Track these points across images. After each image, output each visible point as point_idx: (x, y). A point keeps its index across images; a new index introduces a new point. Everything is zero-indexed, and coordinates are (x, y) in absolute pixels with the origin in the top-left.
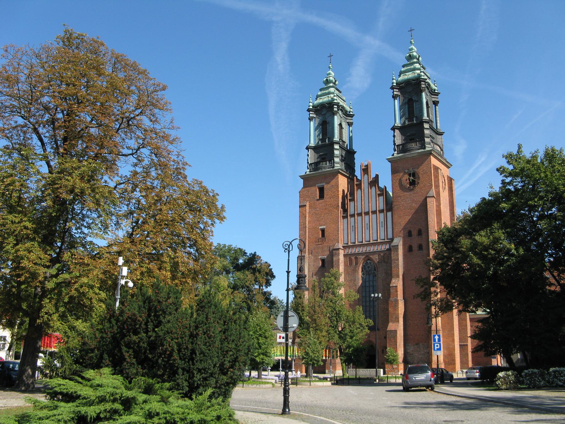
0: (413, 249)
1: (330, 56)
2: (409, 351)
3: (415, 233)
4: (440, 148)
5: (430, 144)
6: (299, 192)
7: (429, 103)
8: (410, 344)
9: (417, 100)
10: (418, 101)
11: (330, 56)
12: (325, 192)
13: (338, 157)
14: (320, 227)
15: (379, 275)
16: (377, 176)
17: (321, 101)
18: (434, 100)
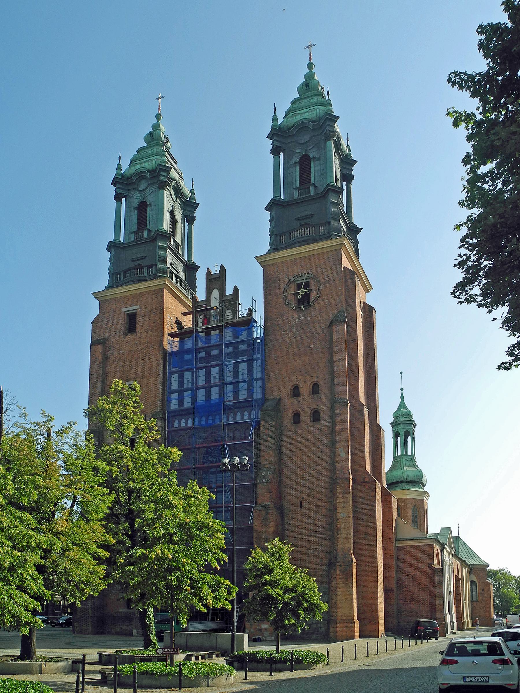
0: (302, 418)
3: (305, 390)
12: (139, 321)
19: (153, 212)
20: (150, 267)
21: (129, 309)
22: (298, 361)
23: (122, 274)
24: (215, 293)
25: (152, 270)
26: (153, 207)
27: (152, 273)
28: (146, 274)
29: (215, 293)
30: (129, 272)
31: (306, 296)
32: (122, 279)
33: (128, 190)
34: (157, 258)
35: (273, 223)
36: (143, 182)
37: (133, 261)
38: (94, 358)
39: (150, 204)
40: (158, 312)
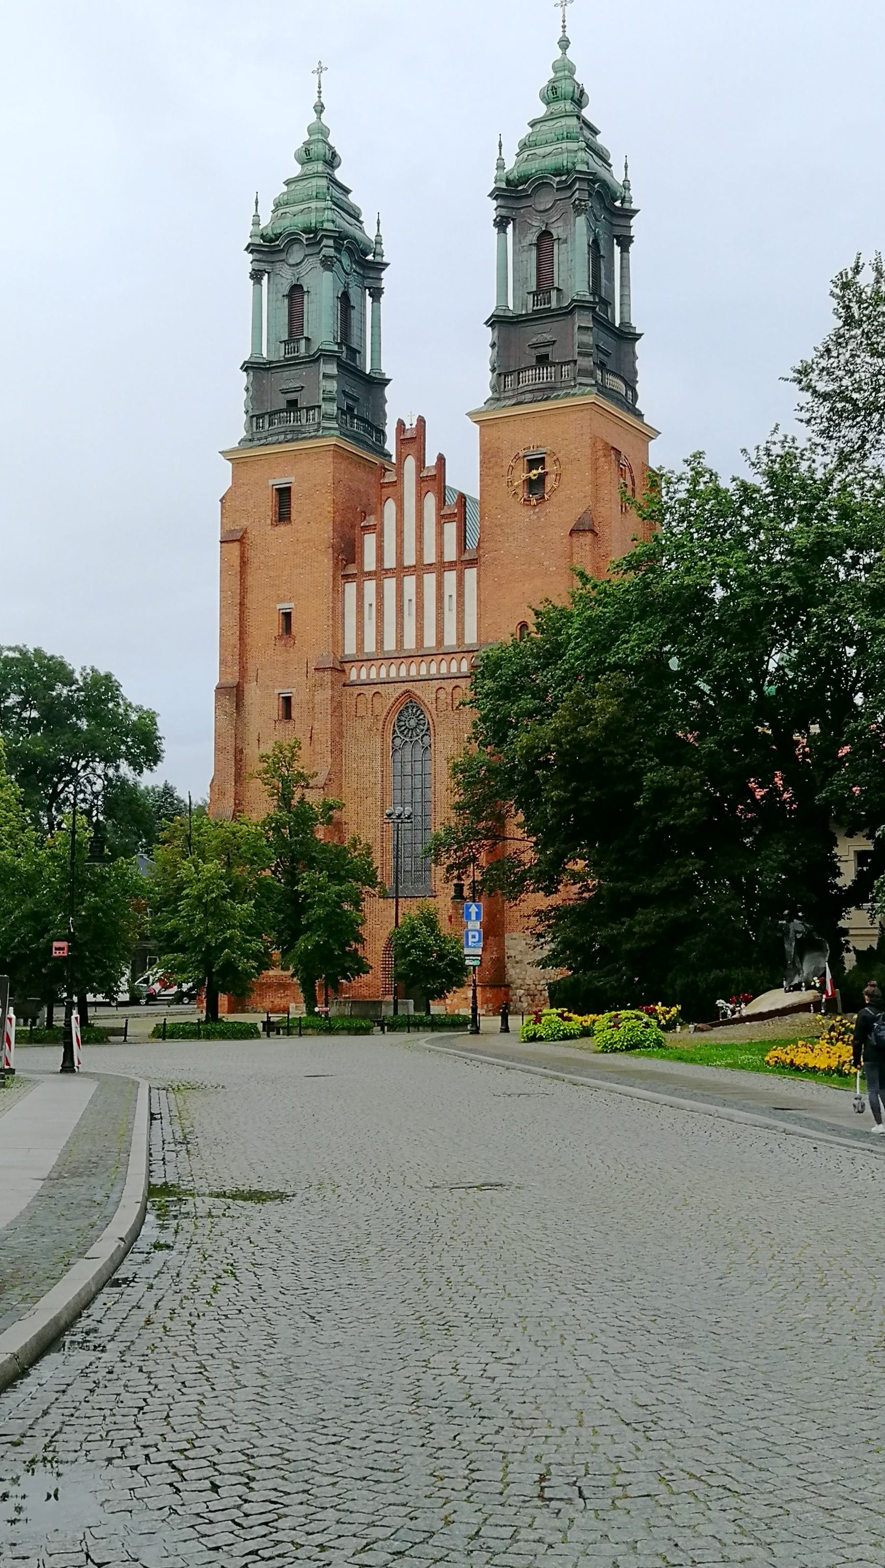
1: (320, 70)
2: (511, 953)
4: (626, 384)
5: (591, 375)
6: (221, 500)
7: (602, 243)
8: (515, 935)
9: (563, 236)
10: (565, 241)
11: (320, 70)
13: (332, 400)
14: (279, 606)
15: (440, 746)
16: (441, 459)
17: (286, 222)
18: (618, 231)
19: (312, 307)
20: (308, 409)
21: (281, 481)
22: (527, 585)
23: (267, 417)
24: (410, 463)
25: (314, 415)
26: (312, 296)
27: (314, 419)
28: (304, 421)
29: (410, 463)
30: (277, 416)
31: (542, 478)
32: (267, 426)
33: (273, 262)
34: (322, 396)
35: (496, 348)
36: (296, 247)
37: (285, 392)
38: (224, 603)
39: (308, 292)
40: (324, 491)
